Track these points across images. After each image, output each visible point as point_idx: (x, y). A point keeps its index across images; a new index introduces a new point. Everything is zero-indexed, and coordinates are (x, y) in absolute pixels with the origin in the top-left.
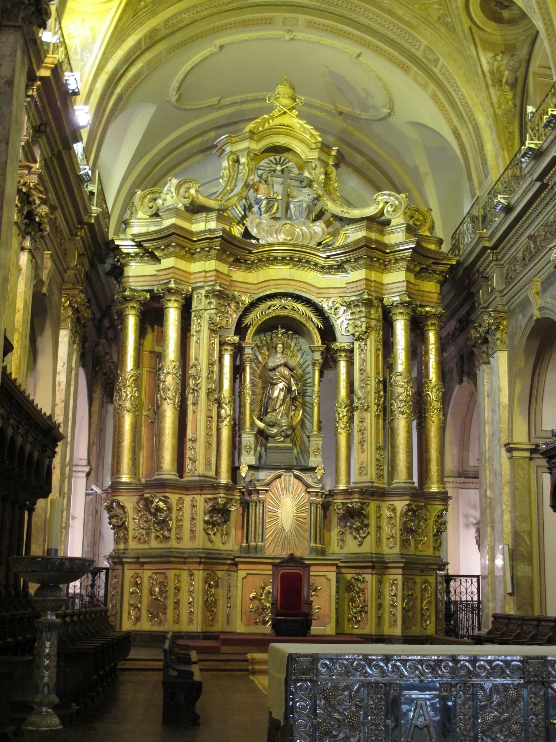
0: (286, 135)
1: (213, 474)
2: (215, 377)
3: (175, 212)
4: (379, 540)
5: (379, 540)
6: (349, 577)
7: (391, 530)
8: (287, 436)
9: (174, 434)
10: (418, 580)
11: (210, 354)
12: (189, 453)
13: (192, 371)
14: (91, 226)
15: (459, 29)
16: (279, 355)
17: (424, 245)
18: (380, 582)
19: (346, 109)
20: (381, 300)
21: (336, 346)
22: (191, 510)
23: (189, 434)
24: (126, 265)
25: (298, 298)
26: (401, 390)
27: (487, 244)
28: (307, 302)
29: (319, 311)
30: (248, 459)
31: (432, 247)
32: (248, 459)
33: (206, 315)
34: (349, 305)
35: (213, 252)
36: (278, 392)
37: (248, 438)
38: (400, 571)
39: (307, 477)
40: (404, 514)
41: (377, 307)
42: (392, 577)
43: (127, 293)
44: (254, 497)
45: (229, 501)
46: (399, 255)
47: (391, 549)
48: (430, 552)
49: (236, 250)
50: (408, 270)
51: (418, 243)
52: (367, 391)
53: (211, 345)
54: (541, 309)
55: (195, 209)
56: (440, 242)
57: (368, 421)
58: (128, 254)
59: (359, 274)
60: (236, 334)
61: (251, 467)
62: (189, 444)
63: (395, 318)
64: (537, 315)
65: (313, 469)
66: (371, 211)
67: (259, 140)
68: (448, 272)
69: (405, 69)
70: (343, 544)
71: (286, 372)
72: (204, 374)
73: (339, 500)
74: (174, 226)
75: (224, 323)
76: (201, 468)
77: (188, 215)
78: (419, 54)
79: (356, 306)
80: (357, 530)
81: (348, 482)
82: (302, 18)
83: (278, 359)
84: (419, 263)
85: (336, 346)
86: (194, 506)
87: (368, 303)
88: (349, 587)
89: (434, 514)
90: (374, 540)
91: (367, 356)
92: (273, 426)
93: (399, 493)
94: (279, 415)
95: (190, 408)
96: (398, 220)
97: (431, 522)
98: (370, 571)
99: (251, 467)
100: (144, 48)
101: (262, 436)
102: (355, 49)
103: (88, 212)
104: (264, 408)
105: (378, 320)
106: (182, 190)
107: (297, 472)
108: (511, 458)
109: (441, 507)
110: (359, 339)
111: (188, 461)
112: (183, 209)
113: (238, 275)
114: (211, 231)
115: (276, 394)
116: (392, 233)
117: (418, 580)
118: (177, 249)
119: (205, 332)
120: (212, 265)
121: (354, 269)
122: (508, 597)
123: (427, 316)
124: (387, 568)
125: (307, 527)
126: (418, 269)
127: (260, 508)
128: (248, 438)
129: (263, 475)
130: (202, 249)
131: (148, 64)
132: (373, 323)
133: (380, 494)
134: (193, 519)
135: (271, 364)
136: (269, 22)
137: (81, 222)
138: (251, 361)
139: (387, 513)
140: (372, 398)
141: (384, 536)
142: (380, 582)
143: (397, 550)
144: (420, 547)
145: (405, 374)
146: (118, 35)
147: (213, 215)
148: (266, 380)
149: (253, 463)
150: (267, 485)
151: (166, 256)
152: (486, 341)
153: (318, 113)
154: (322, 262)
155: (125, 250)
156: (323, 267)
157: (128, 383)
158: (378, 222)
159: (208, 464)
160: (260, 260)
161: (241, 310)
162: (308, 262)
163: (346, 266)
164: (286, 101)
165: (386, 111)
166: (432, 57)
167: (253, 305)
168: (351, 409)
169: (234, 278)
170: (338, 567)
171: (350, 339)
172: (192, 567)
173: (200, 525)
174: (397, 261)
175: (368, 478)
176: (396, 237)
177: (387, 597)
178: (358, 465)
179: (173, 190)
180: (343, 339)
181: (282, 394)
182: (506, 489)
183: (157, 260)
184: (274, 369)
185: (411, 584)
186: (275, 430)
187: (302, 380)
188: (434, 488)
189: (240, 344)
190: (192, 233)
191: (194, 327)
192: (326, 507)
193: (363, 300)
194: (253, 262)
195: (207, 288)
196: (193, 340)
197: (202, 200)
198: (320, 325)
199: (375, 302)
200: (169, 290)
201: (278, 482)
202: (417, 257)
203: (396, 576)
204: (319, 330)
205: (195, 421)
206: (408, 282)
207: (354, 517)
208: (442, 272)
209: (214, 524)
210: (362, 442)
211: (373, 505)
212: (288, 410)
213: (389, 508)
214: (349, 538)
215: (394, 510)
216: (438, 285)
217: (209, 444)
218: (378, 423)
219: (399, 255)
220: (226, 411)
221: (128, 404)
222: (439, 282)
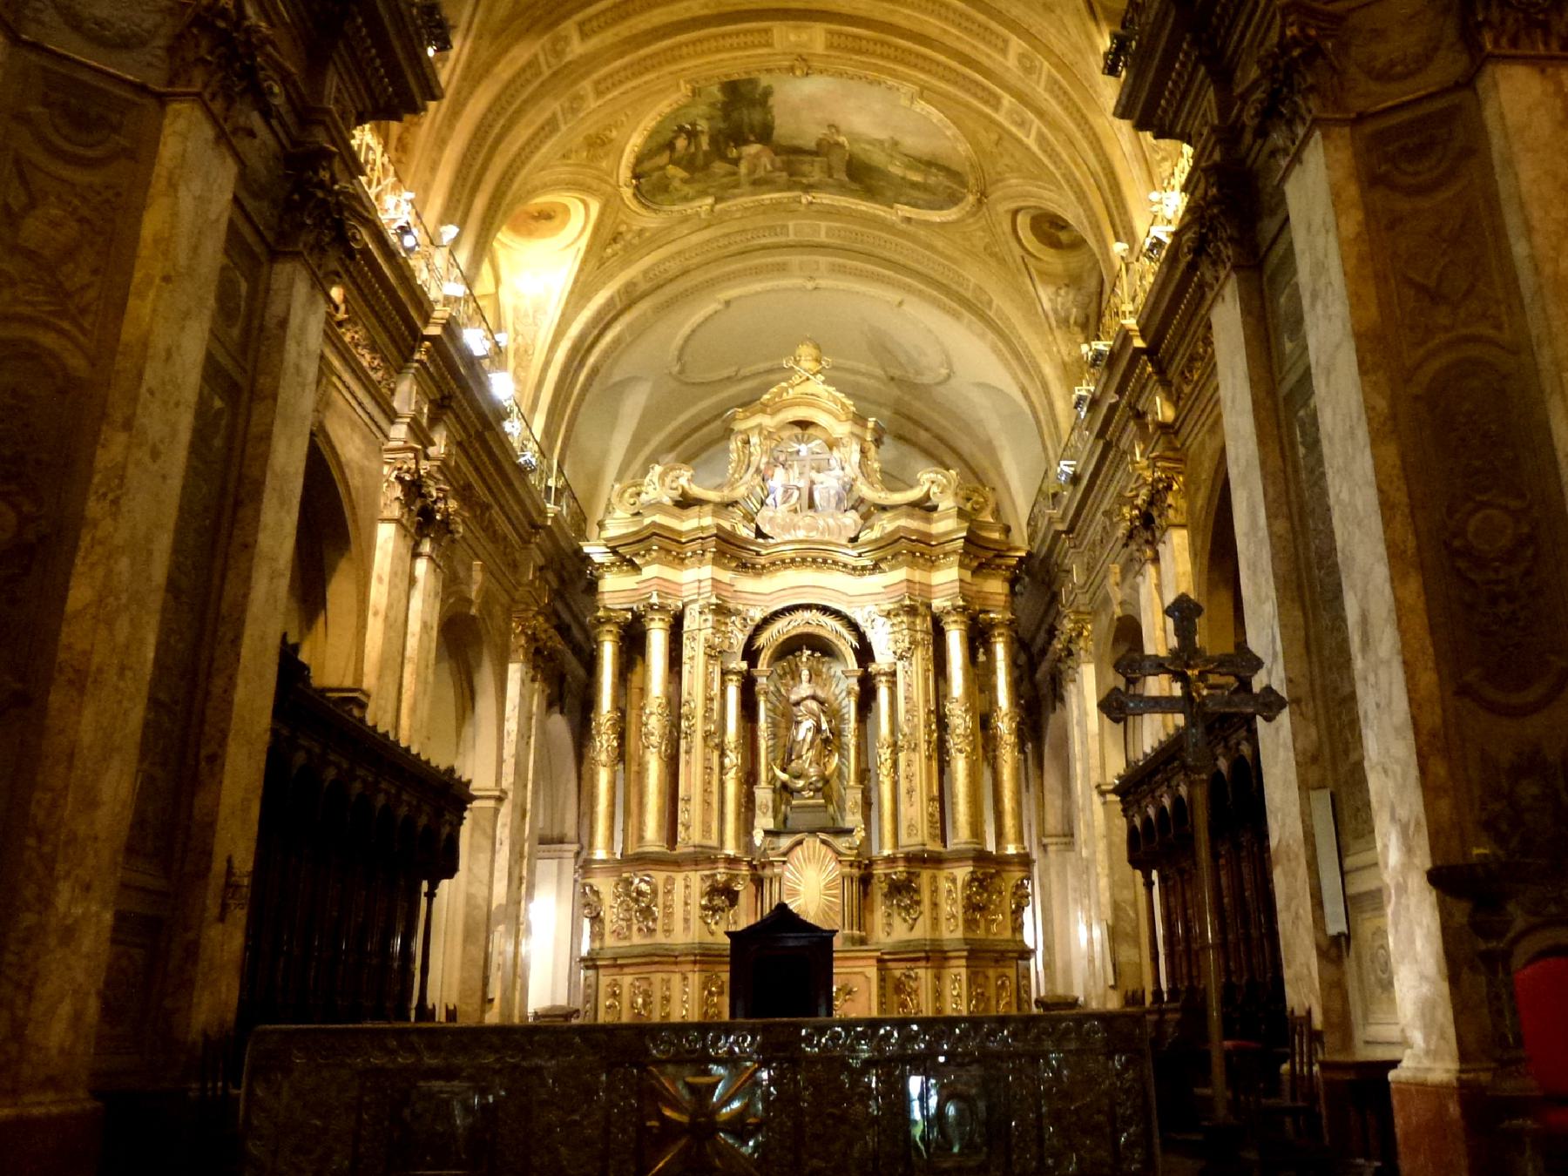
0: (810, 405)
1: (714, 842)
2: (715, 716)
3: (657, 506)
4: (935, 921)
5: (935, 921)
6: (897, 973)
7: (952, 907)
8: (817, 790)
9: (660, 792)
10: (991, 973)
11: (708, 686)
12: (682, 817)
13: (684, 710)
14: (549, 530)
15: (1009, 259)
16: (805, 685)
17: (985, 534)
18: (938, 977)
19: (897, 373)
20: (929, 606)
21: (873, 668)
22: (687, 888)
23: (681, 793)
24: (600, 577)
25: (825, 610)
26: (958, 721)
27: (1061, 527)
28: (837, 614)
29: (853, 626)
30: (764, 821)
31: (996, 536)
32: (764, 821)
33: (701, 636)
34: (888, 615)
35: (709, 556)
36: (804, 731)
38: (963, 962)
39: (842, 843)
40: (969, 884)
41: (925, 617)
42: (955, 971)
43: (601, 613)
44: (768, 872)
45: (733, 878)
46: (948, 547)
47: (952, 933)
48: (1008, 934)
49: (731, 551)
50: (962, 565)
51: (969, 530)
52: (916, 723)
53: (707, 674)
54: (1122, 604)
55: (685, 502)
56: (1007, 530)
57: (917, 765)
58: (602, 564)
59: (901, 574)
60: (743, 659)
61: (767, 833)
62: (681, 805)
63: (947, 628)
64: (1118, 612)
65: (849, 832)
66: (914, 494)
67: (773, 414)
68: (1015, 567)
69: (957, 316)
70: (891, 928)
71: (814, 705)
72: (700, 712)
73: (879, 870)
74: (654, 524)
75: (725, 647)
76: (696, 836)
77: (677, 511)
78: (969, 295)
79: (897, 615)
80: (907, 909)
81: (896, 844)
82: (824, 260)
83: (804, 689)
84: (976, 557)
85: (873, 668)
86: (687, 887)
87: (912, 611)
88: (899, 988)
89: (1013, 882)
90: (928, 922)
91: (913, 678)
92: (798, 777)
93: (959, 857)
94: (806, 761)
95: (683, 757)
96: (947, 503)
97: (1007, 894)
98: (923, 963)
99: (767, 833)
100: (619, 307)
101: (784, 791)
102: (894, 296)
103: (542, 512)
104: (787, 755)
105: (927, 633)
106: (668, 480)
107: (823, 836)
108: (1105, 803)
109: (1021, 875)
110: (901, 658)
111: (680, 828)
112: (670, 503)
114: (702, 529)
115: (800, 738)
116: (941, 520)
117: (991, 973)
118: (663, 554)
119: (701, 659)
120: (707, 571)
121: (892, 568)
122: (1111, 992)
123: (992, 625)
124: (947, 959)
125: (838, 908)
126: (975, 564)
127: (776, 886)
128: (763, 794)
129: (785, 842)
130: (694, 553)
131: (630, 326)
132: (919, 636)
133: (936, 861)
134: (686, 904)
135: (794, 697)
136: (782, 268)
137: (535, 526)
138: (766, 693)
139: (945, 885)
140: (922, 735)
141: (943, 917)
142: (938, 977)
143: (959, 934)
144: (994, 928)
145: (962, 700)
146: (580, 292)
147: (708, 509)
148: (786, 717)
149: (770, 825)
150: (785, 854)
151: (648, 563)
152: (1070, 653)
153: (863, 380)
154: (852, 562)
155: (597, 559)
156: (854, 568)
157: (603, 729)
158: (924, 507)
160: (773, 564)
161: (749, 630)
162: (835, 563)
163: (883, 566)
164: (808, 364)
165: (944, 371)
166: (985, 298)
167: (767, 621)
168: (895, 748)
169: (739, 587)
170: (880, 960)
171: (891, 658)
172: (690, 967)
173: (695, 912)
174: (946, 555)
175: (918, 839)
176: (946, 525)
177: (949, 999)
178: (903, 821)
179: (656, 479)
180: (883, 658)
181: (810, 735)
182: (1102, 846)
183: (636, 569)
184: (797, 704)
185: (981, 980)
186: (800, 783)
187: (835, 715)
188: (1011, 849)
189: (748, 671)
190: (680, 533)
191: (686, 653)
192: (865, 881)
193: (903, 607)
194: (763, 567)
195: (701, 602)
196: (686, 669)
197: (696, 491)
198: (855, 643)
199: (922, 610)
200: (651, 606)
201: (798, 849)
202: (972, 549)
203: (958, 971)
204: (855, 650)
205: (689, 774)
206: (961, 580)
207: (901, 890)
208: (1008, 567)
209: (715, 910)
210: (910, 792)
211: (925, 875)
212: (820, 755)
213: (947, 878)
214: (897, 921)
215: (954, 881)
216: (1007, 585)
217: (707, 803)
218: (929, 767)
219: (948, 547)
220: (733, 759)
221: (603, 757)
222: (1006, 579)
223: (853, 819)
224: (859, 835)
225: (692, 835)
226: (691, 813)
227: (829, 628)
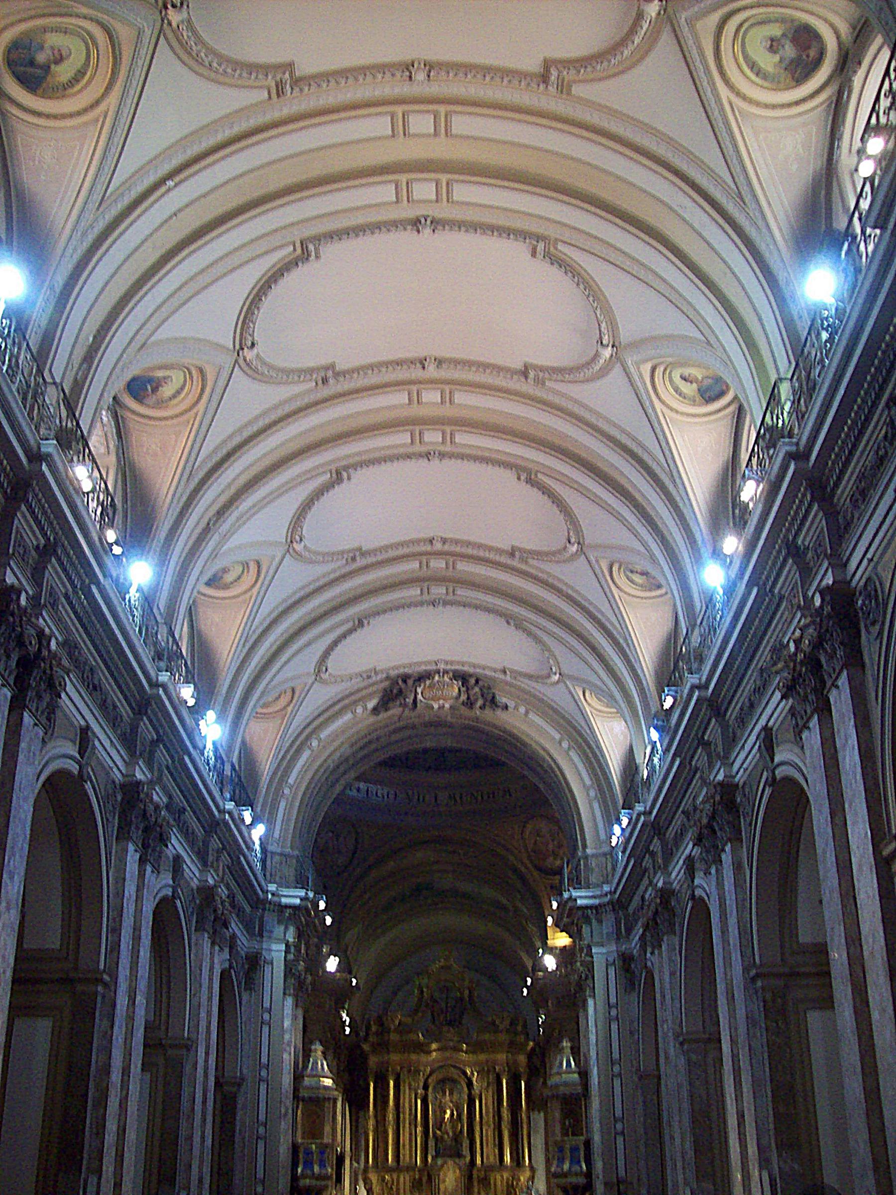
28: (460, 1068)
37: (431, 1143)
59: (482, 1057)
91: (488, 1098)
113: (424, 1058)
128: (431, 1143)
129: (440, 1162)
159: (411, 1157)
217: (411, 1147)
220: (419, 1129)
223: (466, 1152)
224: (468, 1159)
225: (405, 1158)
226: (405, 1152)
227: (454, 1074)
